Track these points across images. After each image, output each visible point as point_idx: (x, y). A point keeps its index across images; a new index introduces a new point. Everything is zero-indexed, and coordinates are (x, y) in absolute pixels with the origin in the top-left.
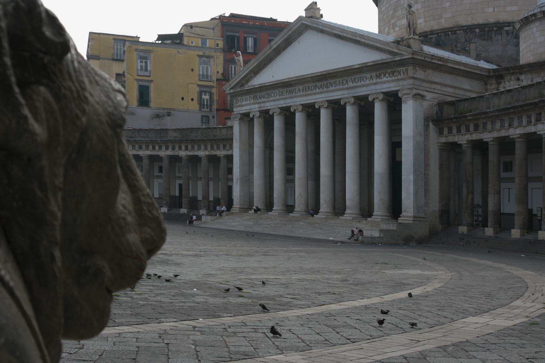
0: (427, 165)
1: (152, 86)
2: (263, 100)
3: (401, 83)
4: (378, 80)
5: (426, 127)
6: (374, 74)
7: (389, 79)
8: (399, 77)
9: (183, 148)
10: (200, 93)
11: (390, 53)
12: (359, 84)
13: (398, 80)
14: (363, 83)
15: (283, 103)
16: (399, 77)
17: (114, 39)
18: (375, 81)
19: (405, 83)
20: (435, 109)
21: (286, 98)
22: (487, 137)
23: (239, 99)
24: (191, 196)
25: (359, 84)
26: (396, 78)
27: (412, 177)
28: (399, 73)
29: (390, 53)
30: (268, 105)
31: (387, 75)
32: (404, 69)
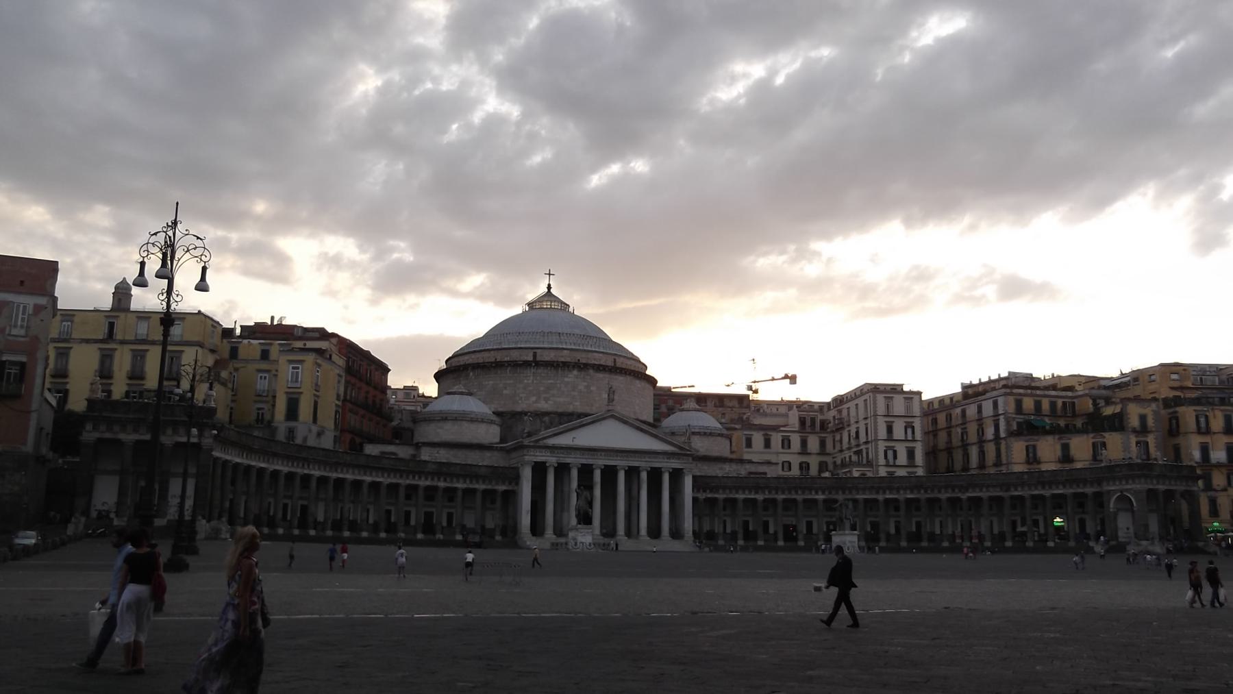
1: (319, 401)
2: (561, 455)
10: (337, 412)
15: (584, 461)
16: (683, 462)
21: (589, 459)
23: (532, 450)
24: (351, 518)
30: (568, 460)
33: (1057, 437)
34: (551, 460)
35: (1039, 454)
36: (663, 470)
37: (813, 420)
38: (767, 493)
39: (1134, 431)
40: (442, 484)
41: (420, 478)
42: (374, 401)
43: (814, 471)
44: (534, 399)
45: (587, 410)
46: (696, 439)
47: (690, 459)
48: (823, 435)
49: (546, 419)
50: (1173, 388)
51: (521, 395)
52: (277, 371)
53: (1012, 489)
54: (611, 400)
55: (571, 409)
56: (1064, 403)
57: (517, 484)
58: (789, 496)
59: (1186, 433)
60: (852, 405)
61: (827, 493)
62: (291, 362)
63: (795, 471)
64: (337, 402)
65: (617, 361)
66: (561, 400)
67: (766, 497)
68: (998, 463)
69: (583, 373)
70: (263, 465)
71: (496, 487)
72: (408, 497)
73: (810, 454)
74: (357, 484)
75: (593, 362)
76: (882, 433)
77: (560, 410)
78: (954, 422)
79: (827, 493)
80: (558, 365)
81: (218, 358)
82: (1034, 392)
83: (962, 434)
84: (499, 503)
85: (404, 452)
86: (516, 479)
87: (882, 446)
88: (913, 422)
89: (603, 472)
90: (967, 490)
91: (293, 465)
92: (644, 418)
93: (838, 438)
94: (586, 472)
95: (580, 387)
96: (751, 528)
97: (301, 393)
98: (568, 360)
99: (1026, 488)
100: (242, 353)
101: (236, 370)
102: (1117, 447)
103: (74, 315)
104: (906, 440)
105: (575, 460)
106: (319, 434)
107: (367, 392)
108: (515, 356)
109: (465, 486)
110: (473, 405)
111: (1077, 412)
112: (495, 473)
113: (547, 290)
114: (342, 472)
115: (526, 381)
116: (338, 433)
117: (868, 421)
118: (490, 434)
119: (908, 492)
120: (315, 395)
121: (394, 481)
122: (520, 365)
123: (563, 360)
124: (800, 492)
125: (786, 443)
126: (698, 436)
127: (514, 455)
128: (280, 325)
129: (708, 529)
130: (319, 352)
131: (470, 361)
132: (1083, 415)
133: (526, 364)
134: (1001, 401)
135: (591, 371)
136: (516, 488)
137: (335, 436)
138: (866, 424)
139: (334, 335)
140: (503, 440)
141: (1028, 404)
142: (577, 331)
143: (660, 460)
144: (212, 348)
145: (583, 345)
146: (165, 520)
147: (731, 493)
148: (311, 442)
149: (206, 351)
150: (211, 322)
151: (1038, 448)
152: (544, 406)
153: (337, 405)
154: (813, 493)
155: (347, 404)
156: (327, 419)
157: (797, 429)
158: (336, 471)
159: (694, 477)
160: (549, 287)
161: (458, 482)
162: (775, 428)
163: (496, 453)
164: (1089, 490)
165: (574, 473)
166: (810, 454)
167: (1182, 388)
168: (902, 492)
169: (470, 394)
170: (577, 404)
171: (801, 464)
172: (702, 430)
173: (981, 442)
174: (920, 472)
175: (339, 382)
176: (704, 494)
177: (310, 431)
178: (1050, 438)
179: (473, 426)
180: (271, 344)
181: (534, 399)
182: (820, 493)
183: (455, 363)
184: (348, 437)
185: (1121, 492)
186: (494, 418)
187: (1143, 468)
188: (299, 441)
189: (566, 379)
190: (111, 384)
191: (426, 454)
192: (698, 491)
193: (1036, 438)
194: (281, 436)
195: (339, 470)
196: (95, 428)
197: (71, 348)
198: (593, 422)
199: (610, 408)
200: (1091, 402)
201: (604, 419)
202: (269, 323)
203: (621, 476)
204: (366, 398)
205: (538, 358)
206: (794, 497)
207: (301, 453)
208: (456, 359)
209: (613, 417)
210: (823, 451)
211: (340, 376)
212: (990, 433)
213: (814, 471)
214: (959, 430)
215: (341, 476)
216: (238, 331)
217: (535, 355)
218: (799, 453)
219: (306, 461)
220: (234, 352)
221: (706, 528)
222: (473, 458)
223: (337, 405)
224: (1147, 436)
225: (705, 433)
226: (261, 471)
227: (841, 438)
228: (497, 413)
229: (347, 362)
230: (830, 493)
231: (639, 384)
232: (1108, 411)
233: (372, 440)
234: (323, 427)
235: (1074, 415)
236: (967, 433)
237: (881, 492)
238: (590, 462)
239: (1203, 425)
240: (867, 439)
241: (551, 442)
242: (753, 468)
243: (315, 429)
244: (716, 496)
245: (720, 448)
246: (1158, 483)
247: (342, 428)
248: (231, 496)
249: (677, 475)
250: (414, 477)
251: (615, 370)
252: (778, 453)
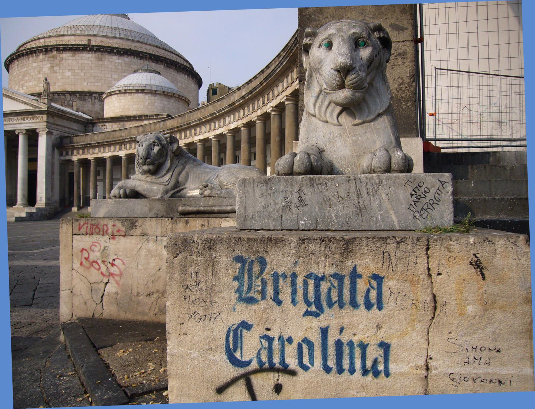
0: (53, 173)
3: (38, 124)
4: (23, 122)
5: (53, 151)
6: (19, 118)
7: (30, 121)
8: (37, 121)
11: (32, 105)
12: (8, 123)
13: (37, 122)
14: (11, 122)
18: (20, 122)
19: (41, 124)
20: (59, 140)
22: (90, 157)
25: (8, 123)
26: (35, 121)
27: (44, 180)
28: (37, 118)
29: (32, 105)
31: (29, 119)
32: (41, 116)
46: (114, 99)
126: (116, 96)
135: (55, 53)
143: (15, 122)
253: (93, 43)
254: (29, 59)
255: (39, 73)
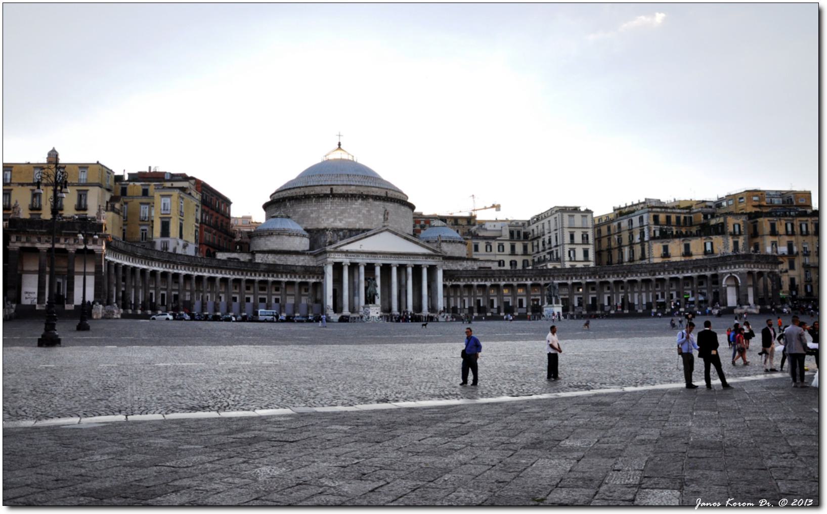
9: (270, 275)
10: (196, 231)
15: (369, 261)
17: (80, 167)
23: (333, 254)
29: (434, 251)
30: (357, 261)
33: (682, 239)
34: (346, 261)
35: (670, 251)
36: (423, 266)
37: (519, 233)
38: (493, 280)
39: (731, 234)
40: (271, 279)
41: (255, 275)
42: (222, 224)
43: (520, 266)
44: (332, 220)
45: (369, 227)
47: (441, 259)
48: (526, 242)
49: (341, 233)
50: (754, 206)
51: (323, 218)
52: (153, 203)
53: (657, 273)
54: (386, 219)
55: (357, 226)
56: (685, 218)
57: (323, 278)
58: (508, 283)
59: (763, 235)
60: (546, 221)
61: (533, 279)
62: (163, 196)
63: (507, 267)
64: (197, 224)
65: (388, 192)
66: (351, 220)
67: (493, 283)
68: (643, 257)
69: (365, 201)
70: (145, 267)
71: (308, 280)
72: (248, 288)
73: (517, 255)
74: (212, 280)
75: (372, 194)
76: (567, 239)
77: (350, 227)
78: (612, 232)
79: (533, 279)
80: (348, 196)
81: (113, 195)
82: (666, 210)
83: (618, 239)
84: (310, 291)
85: (244, 257)
86: (321, 273)
87: (567, 248)
88: (587, 232)
89: (382, 269)
90: (627, 276)
91: (166, 267)
92: (408, 232)
93: (535, 243)
94: (370, 268)
95: (363, 211)
96: (482, 305)
97: (171, 218)
98: (355, 192)
99: (666, 273)
100: (129, 192)
101: (126, 203)
102: (721, 245)
103: (12, 167)
104: (583, 244)
105: (362, 261)
106: (185, 247)
107: (217, 218)
108: (318, 190)
109: (287, 280)
110: (290, 225)
111: (693, 224)
112: (307, 271)
113: (338, 147)
114: (201, 271)
115: (326, 208)
116: (198, 246)
117: (558, 232)
118: (303, 244)
119: (588, 277)
120: (180, 219)
121: (238, 277)
122: (322, 197)
123: (351, 192)
124: (515, 280)
125: (501, 247)
127: (320, 258)
128: (155, 173)
129: (453, 306)
130: (183, 189)
131: (287, 195)
132: (697, 225)
133: (326, 196)
134: (645, 216)
135: (371, 200)
136: (322, 281)
137: (196, 248)
138: (556, 234)
139: (192, 178)
140: (312, 248)
141: (662, 218)
142: (360, 173)
144: (107, 188)
145: (365, 182)
146: (73, 305)
147: (468, 281)
148: (180, 251)
149: (105, 190)
150: (106, 170)
151: (669, 248)
152: (339, 225)
153: (196, 226)
154: (524, 280)
155: (203, 225)
156: (190, 236)
157: (508, 239)
158: (197, 270)
159: (444, 271)
160: (339, 144)
161: (282, 277)
162: (494, 238)
163: (307, 257)
164: (708, 273)
165: (362, 269)
166: (517, 255)
167: (760, 206)
168: (583, 278)
169: (289, 217)
170: (362, 222)
171: (511, 262)
172: (448, 239)
173: (631, 244)
174: (592, 264)
175: (197, 210)
176: (451, 283)
177: (178, 244)
178: (677, 240)
179: (291, 239)
180: (149, 185)
181: (332, 220)
182: (529, 280)
183: (276, 197)
184: (205, 248)
185: (731, 274)
186: (305, 233)
187: (736, 258)
188: (171, 250)
189: (354, 206)
190: (41, 214)
191: (259, 259)
192: (447, 280)
193: (668, 240)
194: (158, 247)
195: (199, 270)
196: (18, 240)
197: (11, 190)
198: (374, 234)
199: (386, 224)
200: (702, 216)
201: (381, 232)
202: (148, 171)
203: (394, 270)
204: (216, 222)
205: (334, 192)
206: (511, 282)
207: (172, 258)
208: (277, 194)
209: (387, 230)
210: (525, 252)
211: (197, 206)
212: (637, 238)
213: (520, 266)
214: (616, 237)
215: (200, 274)
216: (126, 178)
217: (332, 190)
218: (510, 255)
219: (175, 264)
220: (124, 191)
221: (452, 305)
222: (291, 260)
223: (196, 226)
224: (739, 238)
225: (450, 241)
226: (143, 271)
227: (538, 244)
228: (306, 230)
229: (202, 197)
230: (535, 280)
231: (404, 209)
232: (713, 222)
233: (222, 250)
234: (186, 241)
235: (691, 225)
236: (621, 238)
237: (570, 278)
238: (372, 261)
239: (789, 229)
240: (557, 243)
241: (345, 248)
242: (482, 265)
243: (181, 242)
244: (459, 283)
245: (459, 250)
246: (754, 267)
247: (200, 241)
248: (123, 289)
249: (432, 270)
250: (251, 275)
251: (387, 199)
252: (496, 255)
253: (389, 195)
254: (347, 200)
255: (359, 213)
